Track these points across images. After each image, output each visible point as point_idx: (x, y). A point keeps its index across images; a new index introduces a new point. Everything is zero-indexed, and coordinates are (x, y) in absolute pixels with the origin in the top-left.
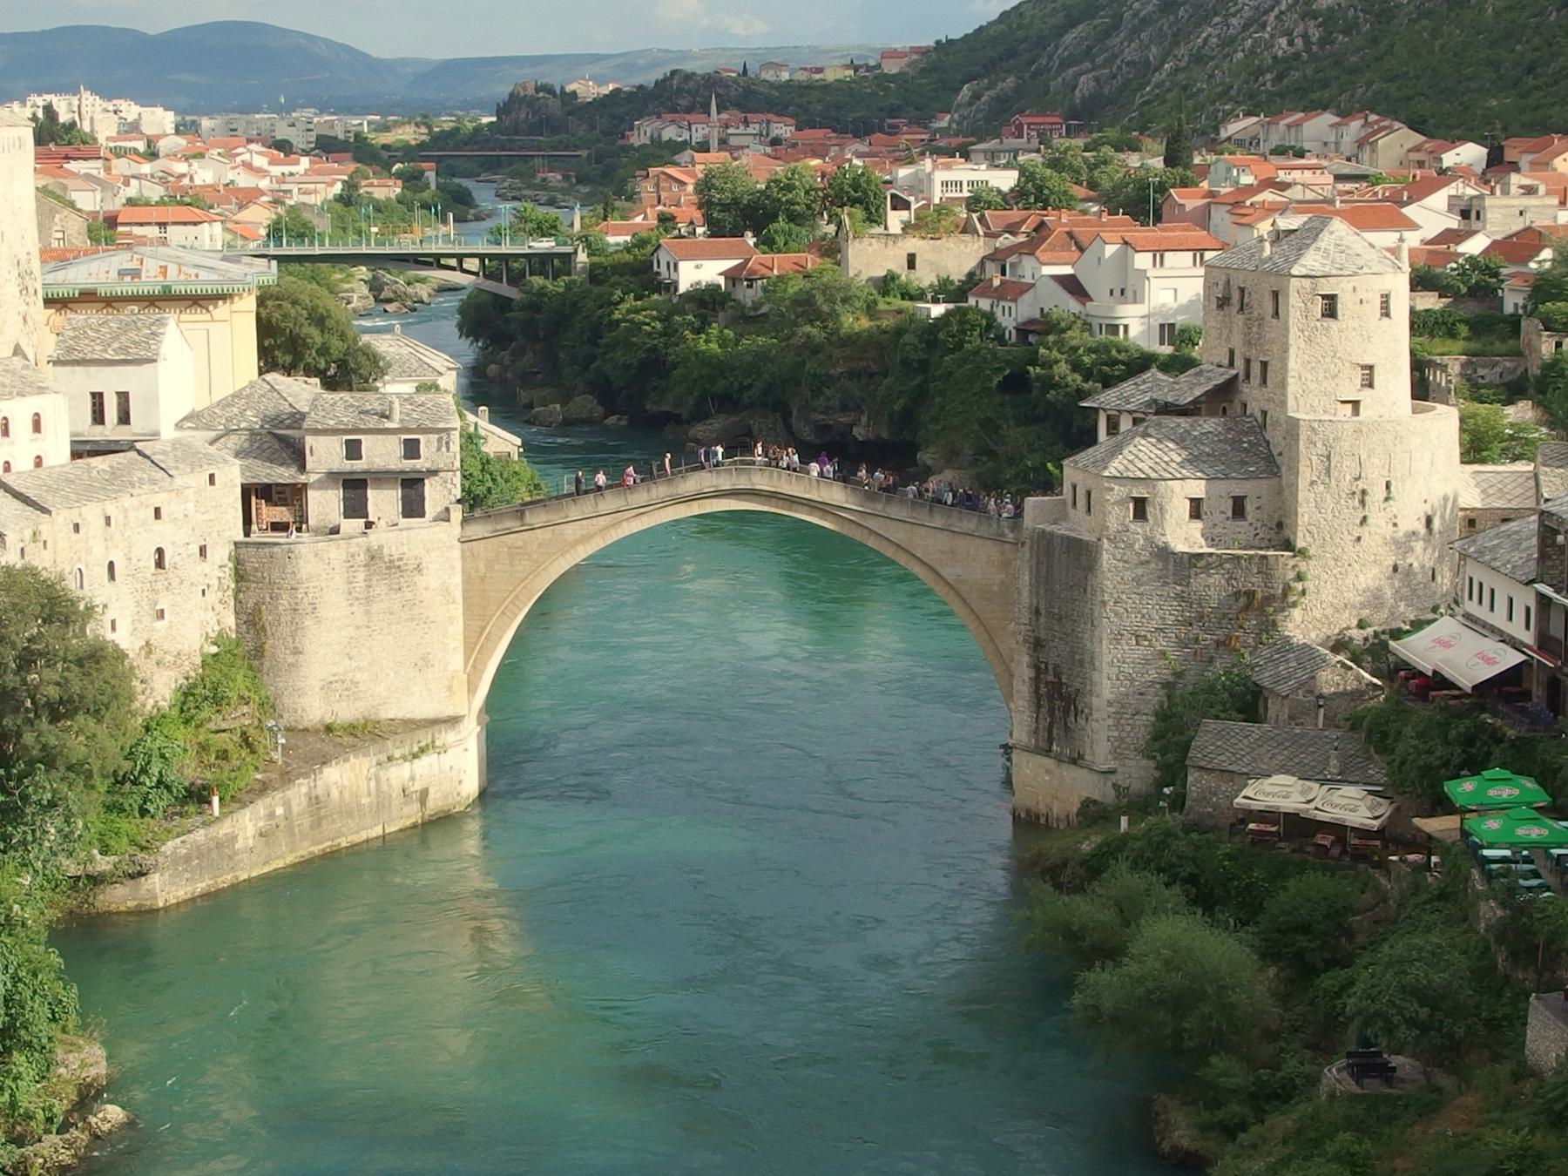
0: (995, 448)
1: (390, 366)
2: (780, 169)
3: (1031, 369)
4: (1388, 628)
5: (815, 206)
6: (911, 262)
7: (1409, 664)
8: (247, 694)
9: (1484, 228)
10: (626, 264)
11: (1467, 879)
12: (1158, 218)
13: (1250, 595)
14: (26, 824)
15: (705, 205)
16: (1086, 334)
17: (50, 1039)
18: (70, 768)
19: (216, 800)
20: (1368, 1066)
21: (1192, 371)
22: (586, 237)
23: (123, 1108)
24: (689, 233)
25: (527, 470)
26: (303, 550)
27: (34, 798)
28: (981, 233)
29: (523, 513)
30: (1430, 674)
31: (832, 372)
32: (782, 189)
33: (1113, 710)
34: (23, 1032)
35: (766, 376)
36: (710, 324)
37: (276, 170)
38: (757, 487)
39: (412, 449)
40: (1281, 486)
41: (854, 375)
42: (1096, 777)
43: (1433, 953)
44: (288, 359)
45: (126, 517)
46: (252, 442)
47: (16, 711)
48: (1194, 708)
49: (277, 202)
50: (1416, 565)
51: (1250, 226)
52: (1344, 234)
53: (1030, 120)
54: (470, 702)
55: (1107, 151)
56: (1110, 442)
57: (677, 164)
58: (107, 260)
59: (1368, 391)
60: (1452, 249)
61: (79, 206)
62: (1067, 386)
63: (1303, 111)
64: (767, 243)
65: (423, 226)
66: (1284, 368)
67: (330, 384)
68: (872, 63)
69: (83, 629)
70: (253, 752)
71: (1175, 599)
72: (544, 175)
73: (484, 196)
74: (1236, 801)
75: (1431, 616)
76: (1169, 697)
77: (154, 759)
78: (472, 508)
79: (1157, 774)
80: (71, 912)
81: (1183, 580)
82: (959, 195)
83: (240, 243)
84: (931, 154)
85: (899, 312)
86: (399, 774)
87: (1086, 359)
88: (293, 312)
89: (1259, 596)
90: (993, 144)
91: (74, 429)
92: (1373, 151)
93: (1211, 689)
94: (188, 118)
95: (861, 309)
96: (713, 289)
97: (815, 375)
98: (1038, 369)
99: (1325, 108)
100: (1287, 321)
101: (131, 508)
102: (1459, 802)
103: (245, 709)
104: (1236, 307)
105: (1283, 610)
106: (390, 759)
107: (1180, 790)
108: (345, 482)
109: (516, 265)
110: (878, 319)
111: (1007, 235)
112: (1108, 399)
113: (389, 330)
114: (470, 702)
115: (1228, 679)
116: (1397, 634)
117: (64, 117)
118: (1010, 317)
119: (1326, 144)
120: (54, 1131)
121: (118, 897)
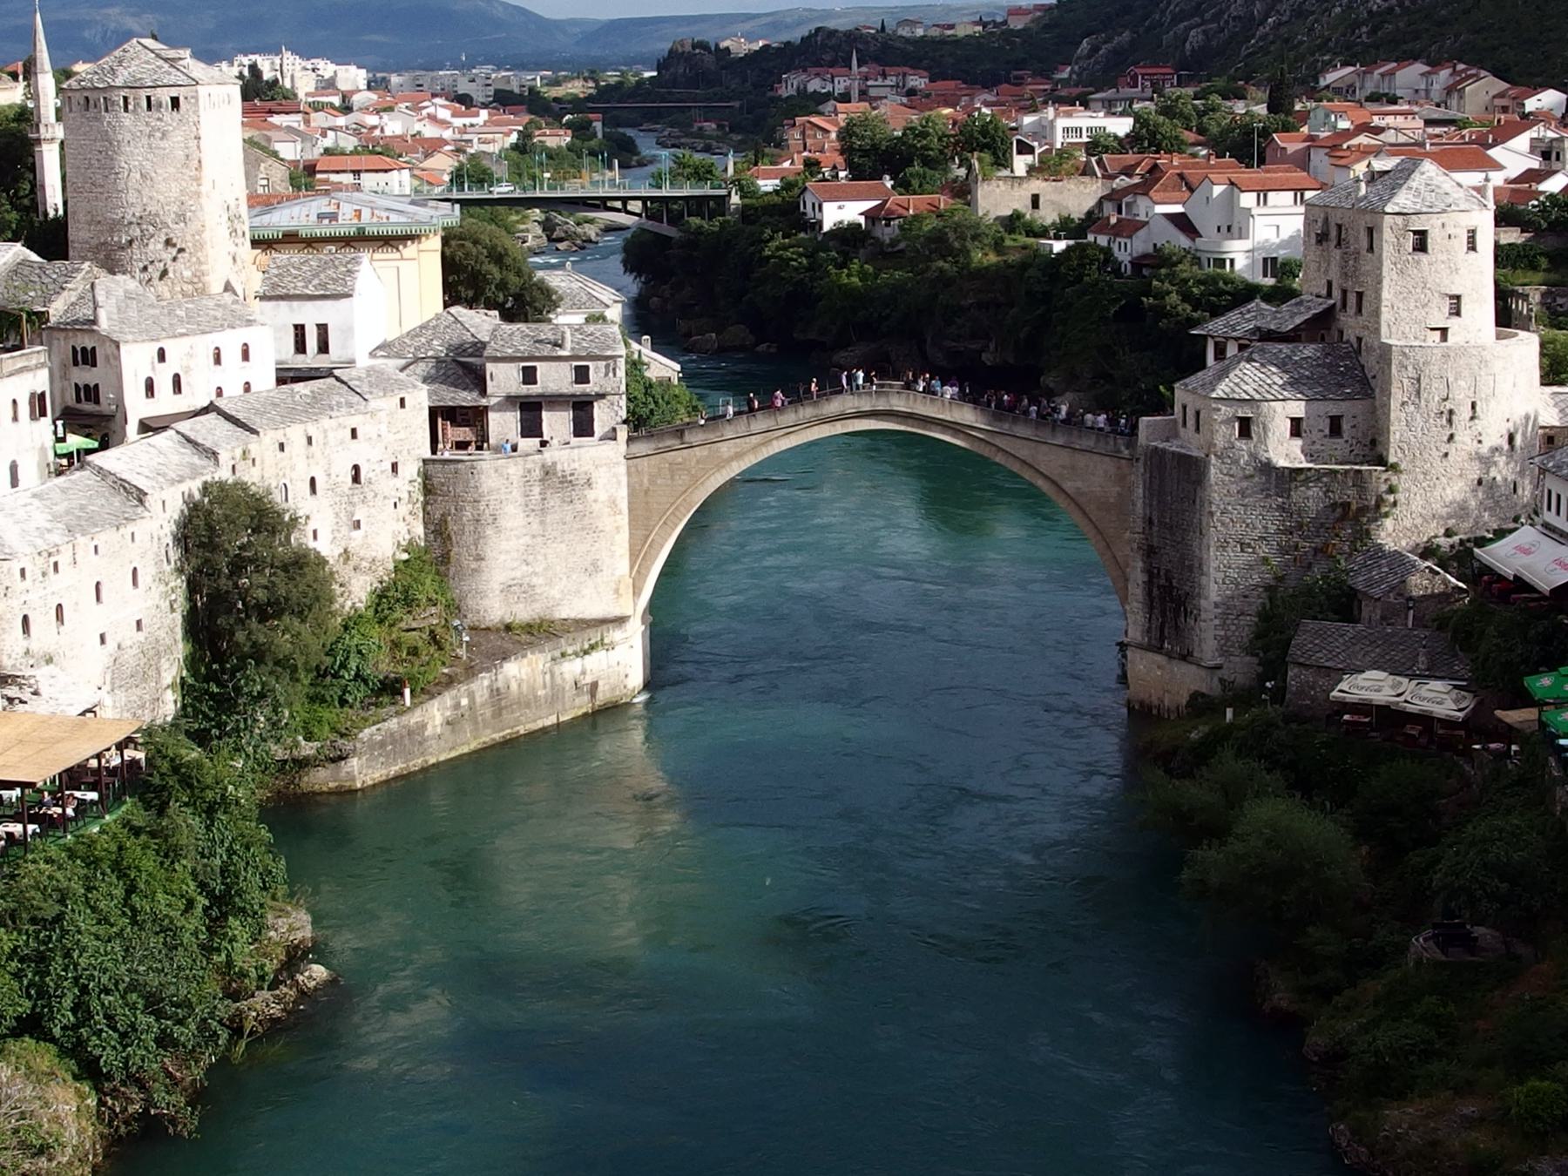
2: (914, 118)
3: (1145, 299)
4: (1472, 536)
5: (948, 152)
8: (435, 596)
10: (774, 205)
12: (1262, 161)
14: (238, 713)
15: (847, 150)
16: (1195, 268)
17: (261, 906)
18: (277, 663)
19: (407, 692)
21: (1293, 301)
22: (739, 180)
25: (685, 394)
27: (246, 690)
28: (1099, 175)
31: (963, 303)
32: (917, 136)
34: (237, 899)
37: (458, 122)
39: (582, 375)
44: (470, 293)
46: (438, 369)
47: (229, 612)
49: (459, 150)
50: (1499, 478)
51: (1347, 167)
54: (635, 604)
56: (1218, 367)
61: (281, 156)
64: (903, 185)
65: (592, 171)
66: (1378, 298)
67: (508, 316)
68: (999, 19)
70: (441, 648)
71: (1276, 510)
73: (646, 145)
77: (352, 655)
78: (636, 428)
80: (279, 792)
83: (426, 188)
84: (1054, 103)
85: (1024, 247)
86: (571, 669)
88: (474, 250)
90: (1110, 93)
94: (379, 75)
95: (989, 245)
96: (854, 227)
98: (1151, 300)
100: (1381, 255)
101: (330, 429)
103: (433, 610)
104: (1335, 242)
106: (563, 655)
108: (522, 404)
109: (675, 207)
110: (1004, 254)
113: (561, 266)
114: (635, 604)
117: (267, 75)
118: (1126, 251)
121: (321, 779)
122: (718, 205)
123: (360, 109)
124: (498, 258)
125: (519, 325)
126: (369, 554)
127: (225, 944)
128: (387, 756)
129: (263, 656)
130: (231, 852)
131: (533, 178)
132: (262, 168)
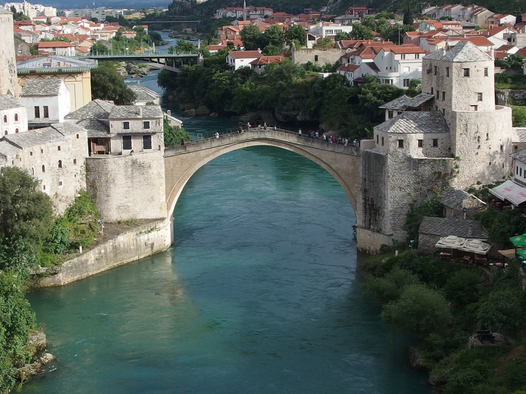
0: (347, 123)
1: (137, 96)
3: (359, 95)
6: (316, 58)
7: (495, 196)
9: (516, 45)
10: (217, 60)
11: (518, 271)
12: (402, 42)
13: (440, 173)
14: (16, 257)
16: (378, 83)
17: (27, 331)
18: (31, 237)
19: (81, 247)
20: (485, 336)
22: (202, 51)
23: (53, 355)
24: (238, 49)
25: (185, 133)
26: (109, 161)
28: (341, 48)
29: (186, 147)
30: (503, 200)
32: (271, 33)
33: (392, 213)
34: (17, 329)
35: (266, 99)
36: (246, 81)
37: (93, 28)
38: (267, 137)
39: (147, 125)
40: (450, 135)
41: (297, 98)
42: (386, 237)
43: (507, 297)
45: (48, 150)
46: (91, 123)
47: (12, 217)
48: (421, 213)
49: (93, 39)
51: (434, 45)
52: (471, 47)
53: (355, 8)
55: (383, 19)
57: (232, 25)
58: (39, 60)
59: (480, 102)
60: (505, 52)
61: (26, 42)
62: (372, 101)
63: (451, 4)
64: (266, 52)
65: (144, 47)
67: (117, 103)
69: (34, 188)
70: (93, 231)
72: (185, 29)
74: (436, 245)
75: (502, 180)
76: (412, 209)
77: (59, 234)
79: (408, 236)
80: (31, 287)
81: (416, 168)
82: (332, 35)
85: (312, 76)
86: (144, 238)
87: (378, 92)
89: (443, 173)
91: (29, 119)
92: (476, 18)
93: (426, 206)
96: (247, 68)
97: (283, 98)
98: (361, 95)
99: (459, 4)
101: (50, 146)
102: (515, 244)
103: (90, 216)
105: (451, 178)
106: (141, 233)
107: (416, 241)
108: (123, 136)
110: (305, 78)
111: (349, 49)
112: (389, 105)
114: (168, 213)
115: (432, 202)
116: (491, 186)
118: (351, 77)
119: (459, 16)
120: (29, 362)
121: (48, 282)
122: (194, 60)
123: (54, 24)
124: (113, 80)
125: (122, 106)
126: (65, 195)
127: (13, 346)
128: (73, 273)
129: (25, 234)
130: (15, 310)
131: (122, 50)
132: (19, 46)
